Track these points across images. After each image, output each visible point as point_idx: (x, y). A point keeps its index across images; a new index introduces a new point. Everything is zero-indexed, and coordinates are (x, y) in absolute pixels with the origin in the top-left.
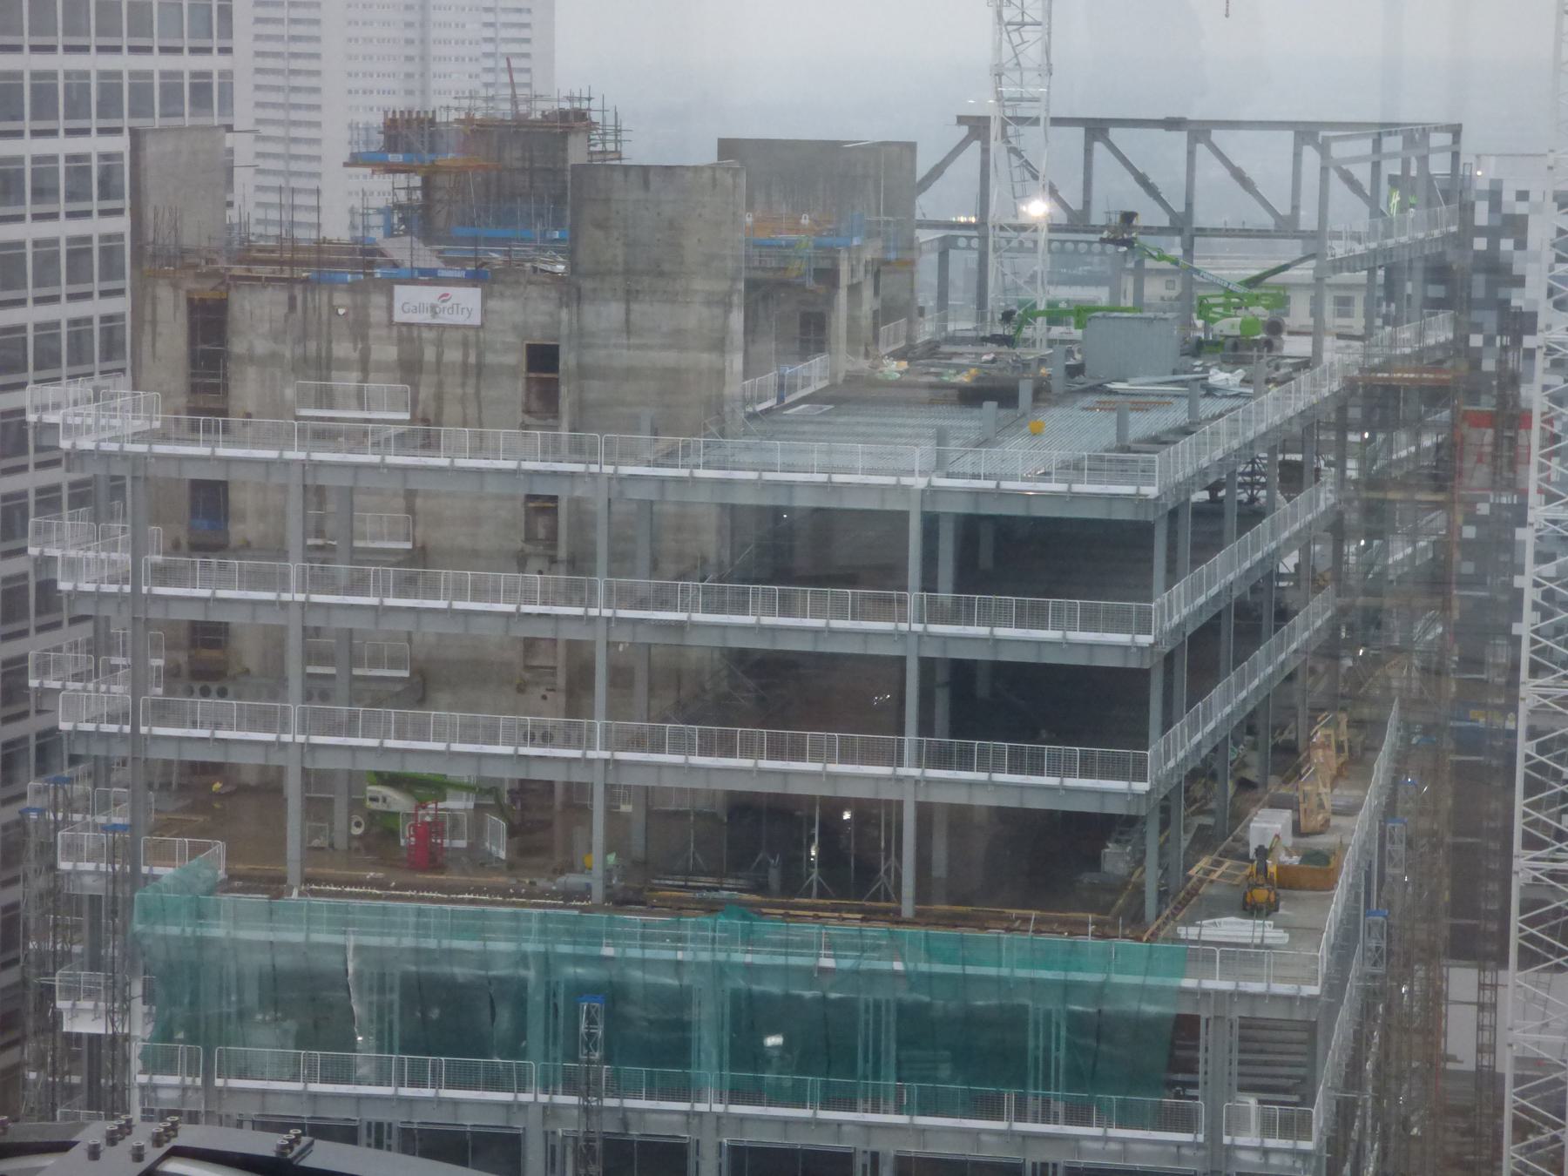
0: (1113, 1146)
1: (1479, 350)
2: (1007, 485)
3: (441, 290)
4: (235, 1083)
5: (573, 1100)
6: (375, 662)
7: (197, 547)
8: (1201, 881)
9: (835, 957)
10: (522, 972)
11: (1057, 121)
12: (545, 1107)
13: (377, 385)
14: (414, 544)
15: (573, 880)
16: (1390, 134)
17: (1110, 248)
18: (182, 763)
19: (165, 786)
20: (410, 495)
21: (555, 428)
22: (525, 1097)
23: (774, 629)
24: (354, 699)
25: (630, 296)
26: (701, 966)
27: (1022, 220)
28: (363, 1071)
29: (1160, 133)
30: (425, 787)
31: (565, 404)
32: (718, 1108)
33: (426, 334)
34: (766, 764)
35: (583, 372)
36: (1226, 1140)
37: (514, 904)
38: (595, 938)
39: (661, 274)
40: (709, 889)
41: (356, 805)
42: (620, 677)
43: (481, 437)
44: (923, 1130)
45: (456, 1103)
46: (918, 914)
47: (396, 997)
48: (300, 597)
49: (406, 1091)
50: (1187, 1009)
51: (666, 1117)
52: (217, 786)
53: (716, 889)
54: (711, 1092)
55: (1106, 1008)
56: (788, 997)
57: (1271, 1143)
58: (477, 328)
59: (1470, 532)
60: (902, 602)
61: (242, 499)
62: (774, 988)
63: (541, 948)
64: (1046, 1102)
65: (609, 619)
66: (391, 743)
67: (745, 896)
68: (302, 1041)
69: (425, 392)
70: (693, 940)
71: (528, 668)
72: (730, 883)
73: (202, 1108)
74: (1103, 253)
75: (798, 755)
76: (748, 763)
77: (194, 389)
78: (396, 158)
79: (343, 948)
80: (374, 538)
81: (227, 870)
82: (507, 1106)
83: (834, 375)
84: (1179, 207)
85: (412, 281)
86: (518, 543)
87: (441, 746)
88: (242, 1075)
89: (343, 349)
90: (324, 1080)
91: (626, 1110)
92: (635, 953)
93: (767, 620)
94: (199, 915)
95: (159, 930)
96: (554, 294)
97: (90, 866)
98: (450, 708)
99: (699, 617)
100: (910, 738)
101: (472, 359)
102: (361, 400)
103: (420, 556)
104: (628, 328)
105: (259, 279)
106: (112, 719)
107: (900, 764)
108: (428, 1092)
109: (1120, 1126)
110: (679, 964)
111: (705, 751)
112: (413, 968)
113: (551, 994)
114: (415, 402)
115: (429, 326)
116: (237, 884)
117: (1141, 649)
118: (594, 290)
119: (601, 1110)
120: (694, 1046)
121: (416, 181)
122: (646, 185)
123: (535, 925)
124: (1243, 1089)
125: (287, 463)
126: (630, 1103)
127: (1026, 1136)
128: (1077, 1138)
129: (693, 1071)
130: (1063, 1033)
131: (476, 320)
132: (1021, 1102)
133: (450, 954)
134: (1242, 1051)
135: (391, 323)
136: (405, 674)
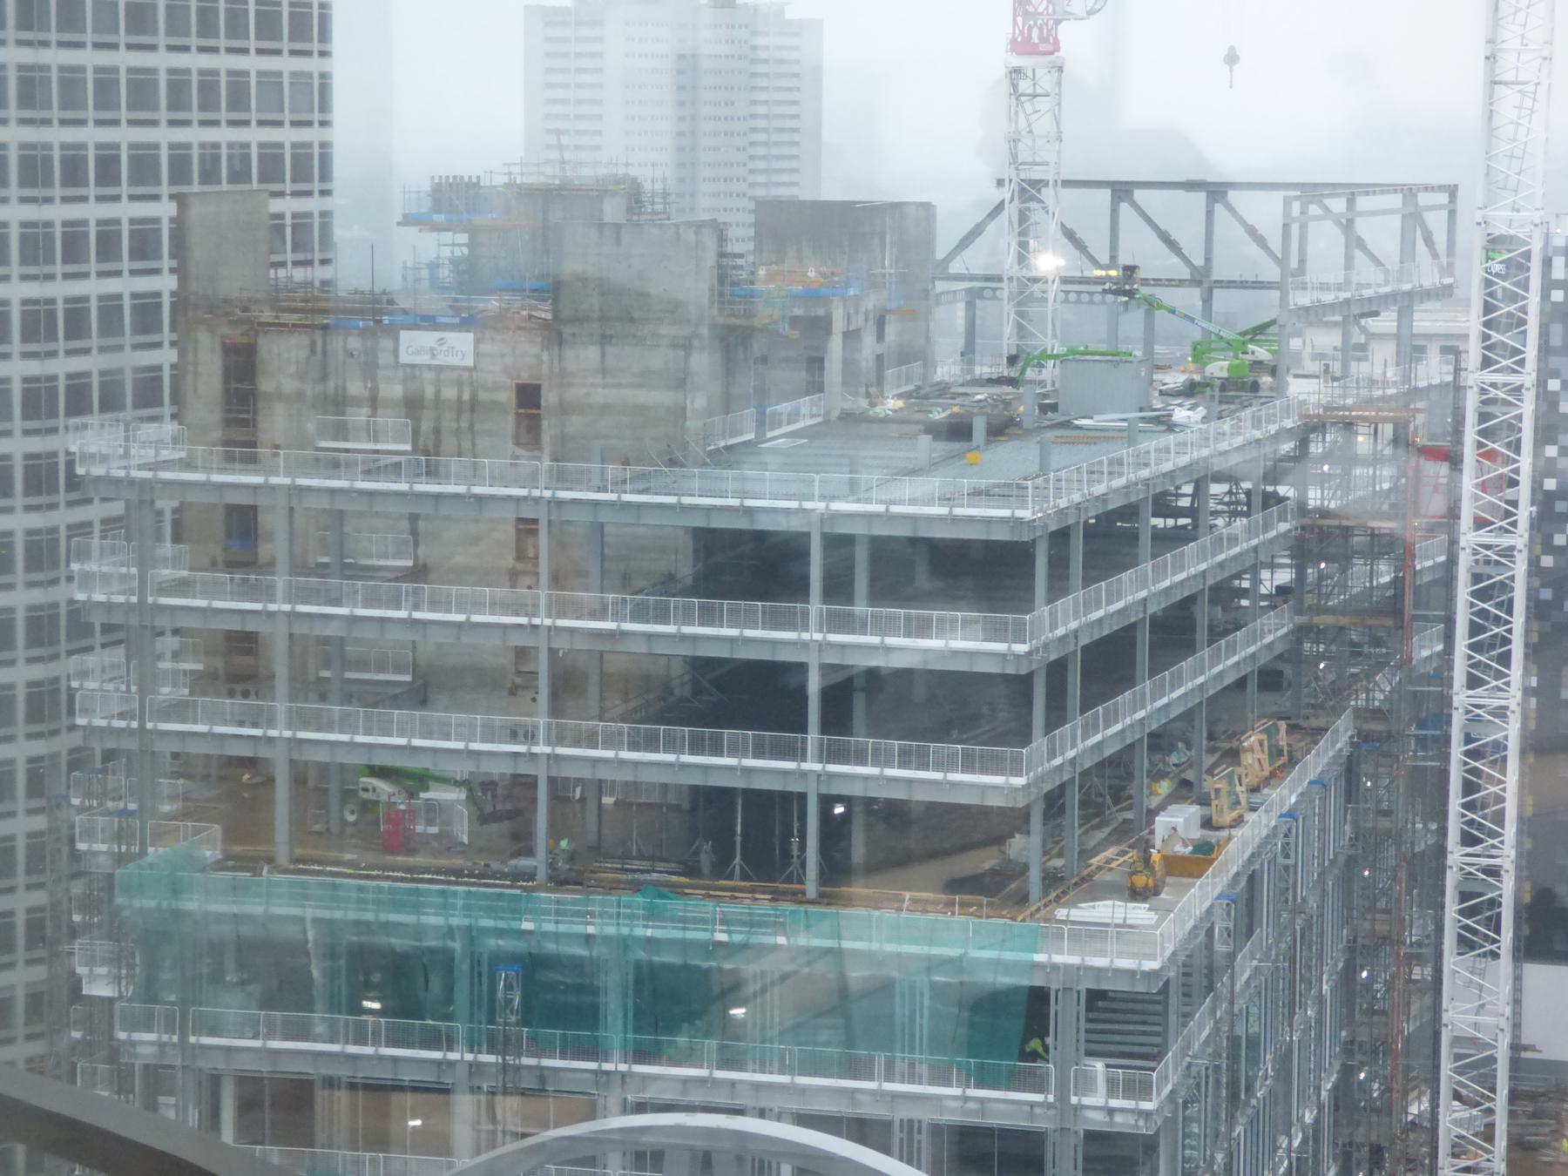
0: (972, 1105)
1: (1555, 393)
2: (895, 509)
3: (437, 335)
4: (207, 1040)
5: (491, 1058)
6: (381, 668)
7: (231, 565)
8: (1100, 868)
9: (729, 932)
10: (450, 944)
11: (1067, 183)
12: (471, 1065)
13: (386, 419)
14: (416, 559)
15: (524, 863)
16: (1367, 193)
17: (1110, 298)
18: (220, 757)
19: (206, 777)
20: (414, 518)
21: (539, 459)
22: (454, 1056)
23: (695, 638)
24: (347, 698)
25: (605, 340)
26: (607, 939)
27: (1034, 274)
28: (319, 1029)
29: (1181, 193)
30: (411, 781)
31: (546, 437)
32: (623, 1067)
33: (428, 375)
34: (687, 758)
35: (564, 409)
36: (1074, 1100)
37: (466, 884)
38: (517, 913)
39: (632, 320)
40: (642, 872)
41: (348, 795)
42: (605, 681)
43: (475, 466)
44: (803, 1091)
45: (395, 1060)
46: (822, 895)
47: (342, 963)
48: (286, 607)
49: (352, 1049)
50: (1038, 981)
51: (578, 1075)
52: (246, 777)
53: (647, 872)
54: (616, 1054)
55: (966, 978)
56: (686, 968)
57: (1115, 1103)
58: (470, 370)
59: (1547, 561)
60: (805, 614)
61: (272, 522)
62: (672, 958)
63: (466, 922)
64: (912, 1065)
65: (549, 628)
66: (360, 739)
67: (675, 878)
68: (268, 1002)
69: (426, 426)
70: (601, 915)
71: (519, 673)
72: (661, 866)
73: (178, 1062)
74: (1103, 302)
75: (717, 750)
76: (670, 757)
77: (228, 423)
78: (439, 218)
79: (302, 920)
80: (379, 557)
81: (224, 851)
82: (438, 1063)
83: (827, 413)
84: (1199, 261)
85: (415, 327)
86: (509, 561)
87: (402, 741)
88: (213, 1032)
89: (356, 387)
90: (286, 1038)
91: (542, 1068)
92: (549, 927)
93: (688, 630)
94: (176, 890)
95: (137, 903)
96: (539, 340)
97: (103, 847)
98: (447, 709)
99: (628, 626)
100: (813, 736)
101: (466, 396)
102: (374, 434)
103: (419, 573)
104: (604, 371)
105: (285, 325)
106: (121, 716)
107: (804, 759)
108: (368, 1050)
109: (977, 1086)
110: (589, 938)
111: (634, 746)
112: (354, 938)
113: (475, 962)
114: (416, 434)
115: (429, 367)
116: (231, 863)
117: (1018, 657)
118: (574, 335)
119: (518, 1068)
120: (602, 1008)
121: (463, 238)
122: (618, 241)
123: (460, 903)
124: (1089, 1054)
125: (273, 488)
126: (547, 1062)
127: (895, 1096)
128: (939, 1098)
129: (601, 1033)
130: (926, 1002)
131: (470, 362)
132: (890, 1065)
133: (387, 927)
134: (1088, 1020)
135: (397, 364)
136: (408, 678)
